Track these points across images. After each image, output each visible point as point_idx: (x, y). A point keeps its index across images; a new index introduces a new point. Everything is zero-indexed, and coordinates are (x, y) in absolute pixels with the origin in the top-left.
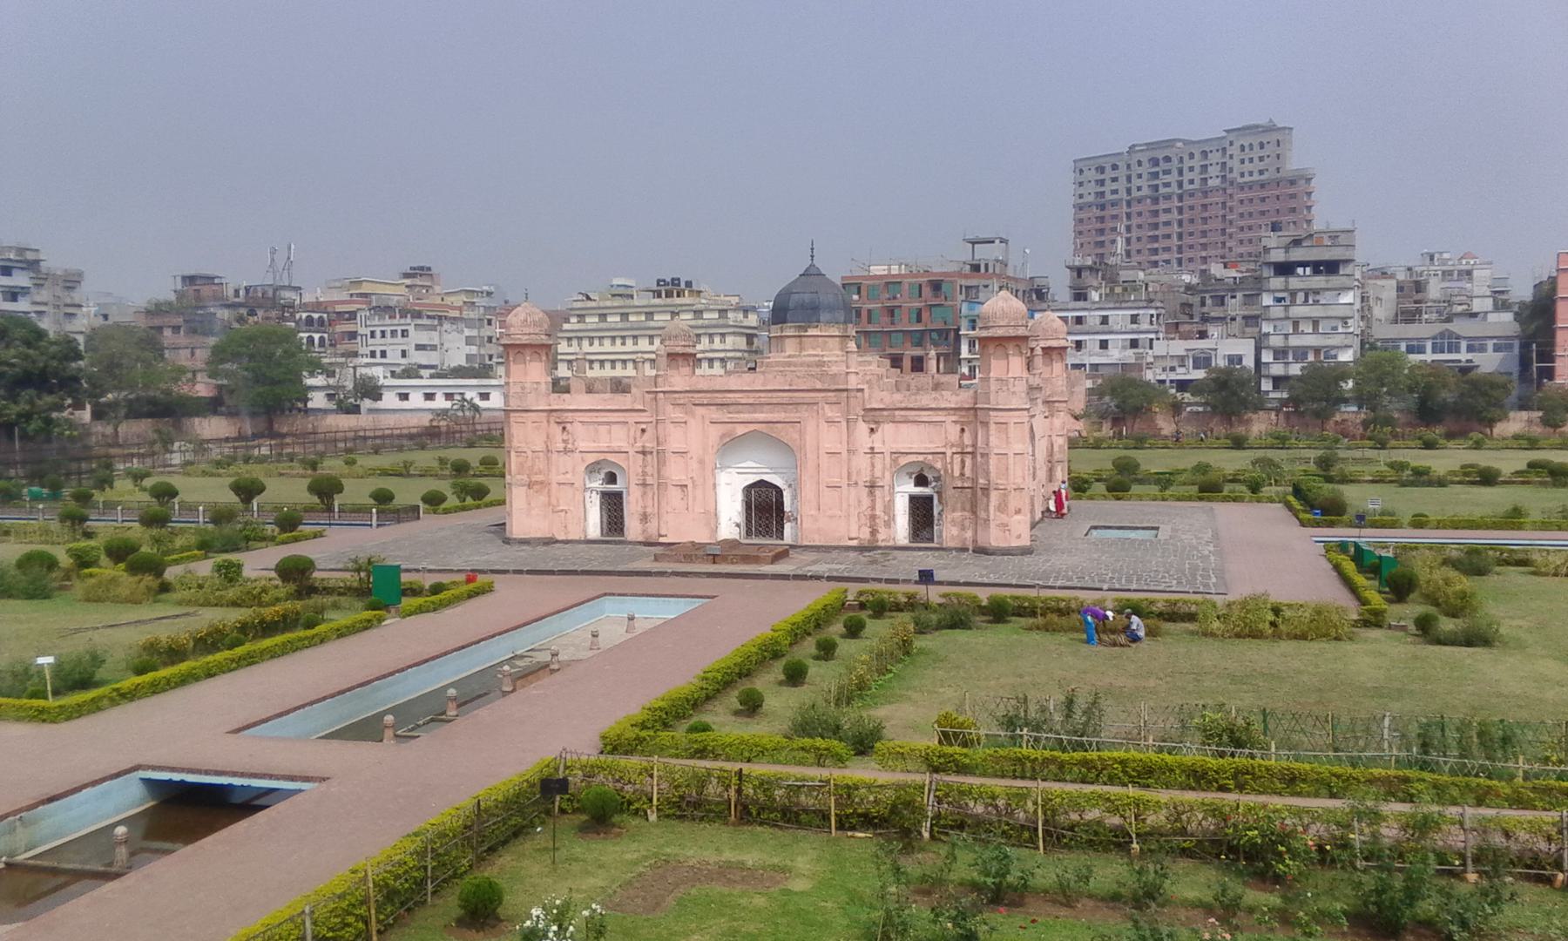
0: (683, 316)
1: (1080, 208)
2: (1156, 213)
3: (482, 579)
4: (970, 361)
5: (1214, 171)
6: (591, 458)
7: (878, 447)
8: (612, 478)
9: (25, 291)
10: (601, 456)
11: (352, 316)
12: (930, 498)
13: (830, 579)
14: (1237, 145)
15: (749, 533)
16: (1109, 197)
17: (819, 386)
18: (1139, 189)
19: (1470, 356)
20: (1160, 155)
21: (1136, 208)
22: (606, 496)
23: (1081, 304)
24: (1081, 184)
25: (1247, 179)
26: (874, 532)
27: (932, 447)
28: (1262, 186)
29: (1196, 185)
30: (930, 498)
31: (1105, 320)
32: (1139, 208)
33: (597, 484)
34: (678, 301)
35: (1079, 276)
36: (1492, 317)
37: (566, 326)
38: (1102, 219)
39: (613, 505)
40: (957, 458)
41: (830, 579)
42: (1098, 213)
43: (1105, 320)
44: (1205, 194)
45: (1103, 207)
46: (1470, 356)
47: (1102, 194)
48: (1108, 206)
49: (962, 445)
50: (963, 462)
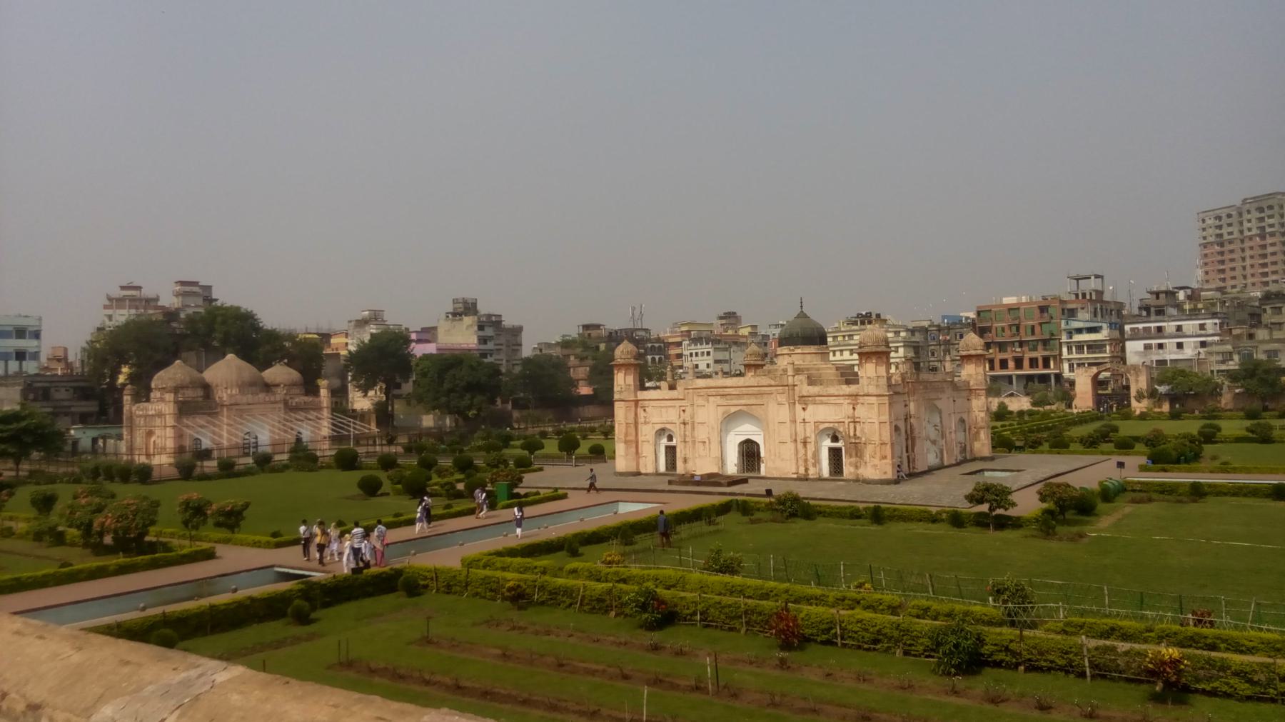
2: (1264, 247)
3: (560, 492)
4: (1069, 360)
6: (658, 427)
8: (670, 438)
9: (491, 338)
11: (679, 344)
16: (1226, 237)
17: (773, 383)
18: (1250, 230)
21: (1247, 244)
22: (667, 448)
24: (1204, 229)
26: (807, 470)
27: (837, 418)
31: (1179, 328)
32: (1251, 244)
35: (1158, 298)
38: (1222, 253)
40: (852, 425)
43: (1179, 328)
47: (1221, 236)
48: (1226, 244)
49: (854, 417)
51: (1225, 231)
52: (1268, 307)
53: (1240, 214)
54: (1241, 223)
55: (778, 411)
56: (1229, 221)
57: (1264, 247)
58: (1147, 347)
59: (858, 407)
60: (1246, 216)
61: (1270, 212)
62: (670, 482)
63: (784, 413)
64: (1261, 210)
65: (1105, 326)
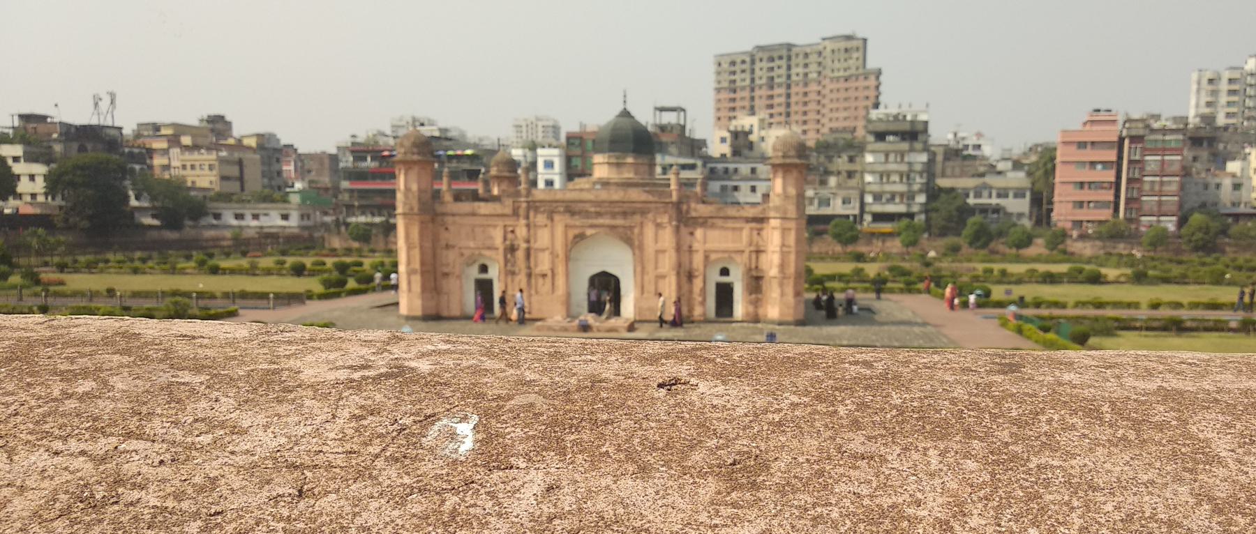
1: (718, 90)
2: (771, 97)
6: (467, 253)
7: (696, 246)
8: (484, 269)
14: (829, 49)
23: (737, 158)
25: (836, 74)
31: (753, 170)
33: (474, 273)
39: (484, 288)
40: (754, 256)
42: (732, 95)
43: (753, 170)
44: (806, 85)
45: (735, 91)
47: (734, 81)
49: (757, 245)
51: (737, 77)
53: (753, 62)
54: (753, 71)
55: (659, 237)
56: (744, 67)
57: (771, 97)
58: (724, 188)
59: (764, 233)
60: (758, 65)
63: (667, 238)
65: (699, 163)
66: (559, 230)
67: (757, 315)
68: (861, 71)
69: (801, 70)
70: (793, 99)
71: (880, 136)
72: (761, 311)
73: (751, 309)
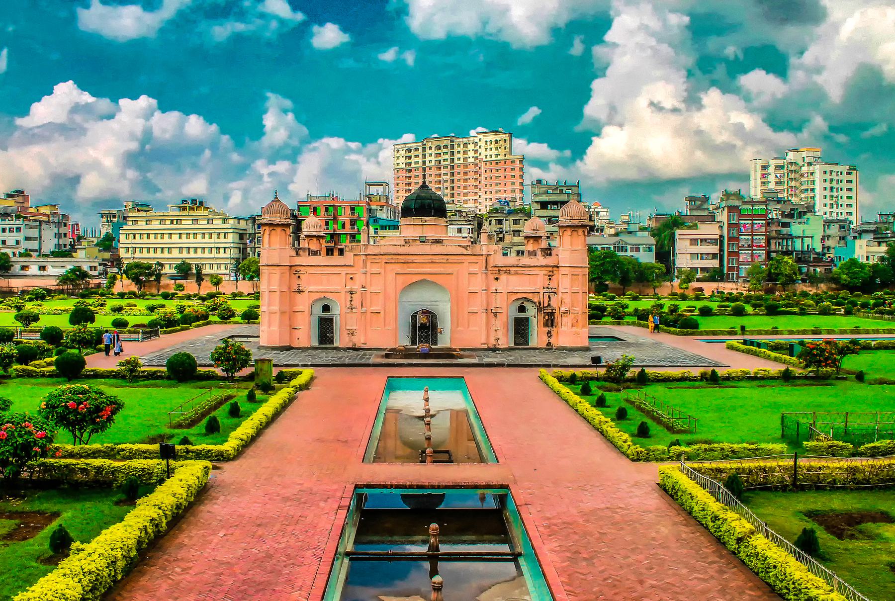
0: (200, 222)
5: (471, 154)
7: (500, 289)
8: (326, 308)
10: (322, 295)
12: (527, 320)
13: (509, 366)
15: (413, 342)
17: (465, 252)
18: (430, 161)
19: (632, 254)
20: (442, 144)
22: (321, 319)
25: (489, 159)
27: (531, 288)
28: (497, 163)
29: (462, 161)
30: (527, 320)
33: (318, 312)
34: (196, 213)
36: (639, 234)
37: (125, 227)
40: (546, 296)
41: (509, 366)
42: (408, 174)
45: (410, 171)
46: (632, 254)
47: (410, 163)
48: (413, 170)
50: (549, 297)
52: (493, 219)
53: (424, 149)
54: (424, 156)
60: (428, 151)
61: (445, 150)
62: (387, 356)
64: (438, 147)
66: (391, 276)
67: (549, 344)
68: (508, 157)
69: (461, 156)
70: (456, 177)
71: (544, 205)
72: (552, 340)
73: (545, 339)
